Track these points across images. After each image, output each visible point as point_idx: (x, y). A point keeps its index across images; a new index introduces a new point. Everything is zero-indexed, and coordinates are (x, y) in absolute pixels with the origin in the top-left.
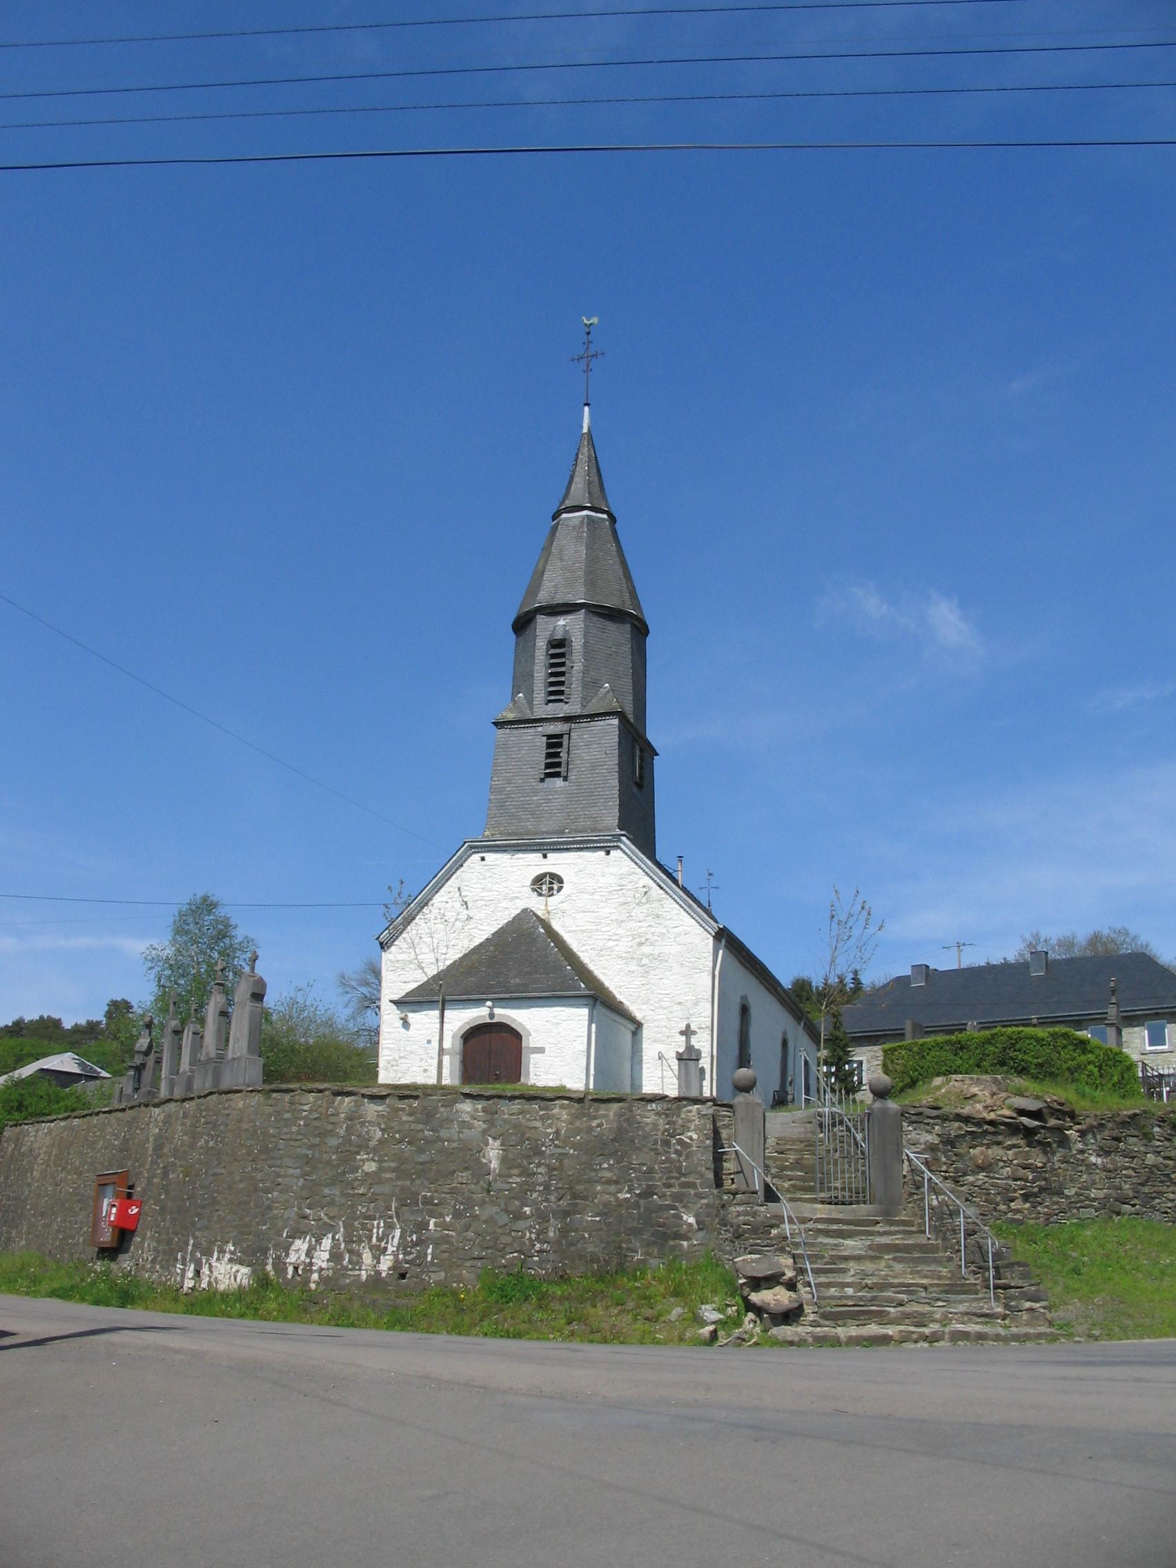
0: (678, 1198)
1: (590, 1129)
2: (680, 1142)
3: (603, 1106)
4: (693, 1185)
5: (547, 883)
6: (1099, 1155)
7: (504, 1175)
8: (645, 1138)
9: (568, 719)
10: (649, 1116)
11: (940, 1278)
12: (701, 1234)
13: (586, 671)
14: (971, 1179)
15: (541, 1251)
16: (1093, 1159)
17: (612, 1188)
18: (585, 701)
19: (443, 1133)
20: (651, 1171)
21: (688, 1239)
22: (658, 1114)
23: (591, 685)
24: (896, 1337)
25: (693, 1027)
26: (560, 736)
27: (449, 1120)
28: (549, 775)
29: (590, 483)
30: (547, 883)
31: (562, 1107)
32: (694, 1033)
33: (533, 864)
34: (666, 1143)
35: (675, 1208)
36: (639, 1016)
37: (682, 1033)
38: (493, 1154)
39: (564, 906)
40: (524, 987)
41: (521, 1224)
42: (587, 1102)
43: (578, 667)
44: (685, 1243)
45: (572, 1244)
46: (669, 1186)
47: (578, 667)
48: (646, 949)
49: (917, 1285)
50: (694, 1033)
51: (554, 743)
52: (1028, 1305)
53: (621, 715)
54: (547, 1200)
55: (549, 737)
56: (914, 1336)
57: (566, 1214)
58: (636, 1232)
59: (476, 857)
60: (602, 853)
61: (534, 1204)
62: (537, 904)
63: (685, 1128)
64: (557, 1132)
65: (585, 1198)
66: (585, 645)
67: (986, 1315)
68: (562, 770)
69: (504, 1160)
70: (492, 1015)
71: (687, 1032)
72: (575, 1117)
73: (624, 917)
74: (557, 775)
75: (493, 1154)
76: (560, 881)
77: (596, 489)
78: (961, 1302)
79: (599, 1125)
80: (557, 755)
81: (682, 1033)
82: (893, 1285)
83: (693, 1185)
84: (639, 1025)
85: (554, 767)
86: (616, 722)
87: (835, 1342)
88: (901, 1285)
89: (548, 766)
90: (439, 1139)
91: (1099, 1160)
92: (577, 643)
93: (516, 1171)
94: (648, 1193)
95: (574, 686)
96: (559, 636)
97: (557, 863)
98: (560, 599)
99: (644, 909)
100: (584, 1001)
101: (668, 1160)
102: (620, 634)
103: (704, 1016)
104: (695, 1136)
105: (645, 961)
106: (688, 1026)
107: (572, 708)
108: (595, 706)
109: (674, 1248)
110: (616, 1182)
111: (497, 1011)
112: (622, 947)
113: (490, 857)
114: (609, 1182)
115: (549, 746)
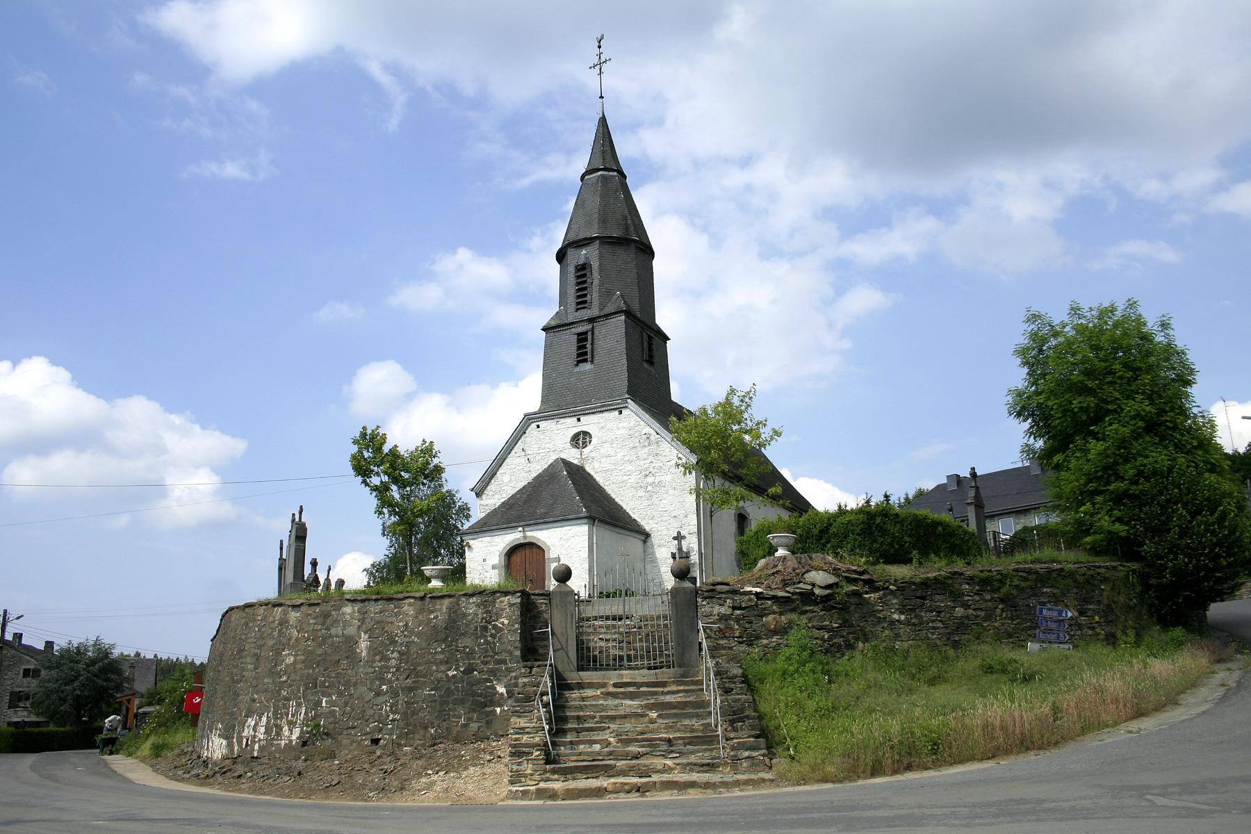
0: (493, 672)
1: (430, 621)
2: (495, 627)
3: (438, 602)
4: (504, 662)
5: (581, 439)
6: (902, 613)
7: (370, 662)
8: (467, 625)
9: (591, 320)
10: (471, 608)
11: (692, 731)
12: (510, 702)
13: (601, 284)
14: (765, 642)
15: (393, 720)
16: (896, 616)
17: (443, 668)
18: (602, 306)
19: (333, 631)
20: (472, 652)
21: (501, 706)
22: (478, 605)
23: (607, 294)
24: (610, 788)
25: (683, 533)
26: (586, 333)
27: (337, 621)
28: (579, 362)
29: (603, 152)
30: (581, 439)
31: (410, 605)
32: (684, 537)
33: (570, 426)
34: (485, 629)
35: (489, 680)
36: (647, 528)
37: (675, 538)
38: (364, 644)
39: (593, 454)
40: (543, 516)
41: (381, 699)
42: (427, 600)
43: (596, 282)
44: (498, 710)
45: (413, 714)
46: (486, 663)
47: (596, 282)
48: (650, 479)
49: (660, 739)
50: (684, 537)
51: (582, 338)
52: (747, 754)
53: (628, 313)
54: (397, 679)
55: (579, 334)
56: (627, 787)
57: (410, 689)
58: (462, 702)
59: (534, 425)
60: (617, 413)
61: (389, 681)
62: (573, 456)
63: (498, 616)
64: (406, 625)
65: (425, 676)
66: (600, 265)
67: (708, 765)
68: (589, 356)
69: (369, 649)
70: (525, 537)
71: (679, 538)
72: (420, 611)
73: (633, 458)
74: (585, 361)
75: (364, 644)
76: (590, 436)
77: (609, 156)
78: (692, 753)
79: (436, 617)
80: (585, 347)
81: (675, 538)
82: (637, 740)
83: (504, 662)
84: (646, 536)
85: (582, 356)
86: (623, 318)
87: (553, 795)
88: (643, 740)
89: (579, 355)
90: (331, 636)
91: (903, 617)
92: (595, 265)
93: (378, 658)
94: (469, 670)
95: (594, 296)
96: (581, 262)
97: (590, 423)
98: (581, 236)
99: (646, 450)
100: (585, 521)
101: (487, 642)
102: (625, 257)
103: (690, 525)
104: (506, 622)
105: (650, 488)
106: (679, 533)
107: (594, 312)
108: (608, 310)
109: (488, 714)
110: (447, 662)
111: (528, 534)
112: (633, 480)
113: (543, 424)
114: (442, 662)
115: (579, 341)
